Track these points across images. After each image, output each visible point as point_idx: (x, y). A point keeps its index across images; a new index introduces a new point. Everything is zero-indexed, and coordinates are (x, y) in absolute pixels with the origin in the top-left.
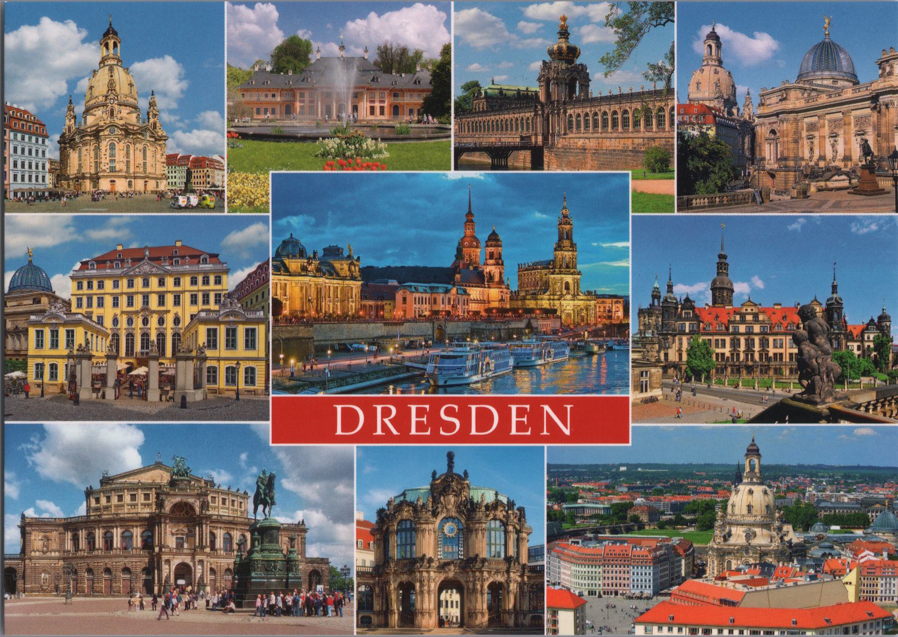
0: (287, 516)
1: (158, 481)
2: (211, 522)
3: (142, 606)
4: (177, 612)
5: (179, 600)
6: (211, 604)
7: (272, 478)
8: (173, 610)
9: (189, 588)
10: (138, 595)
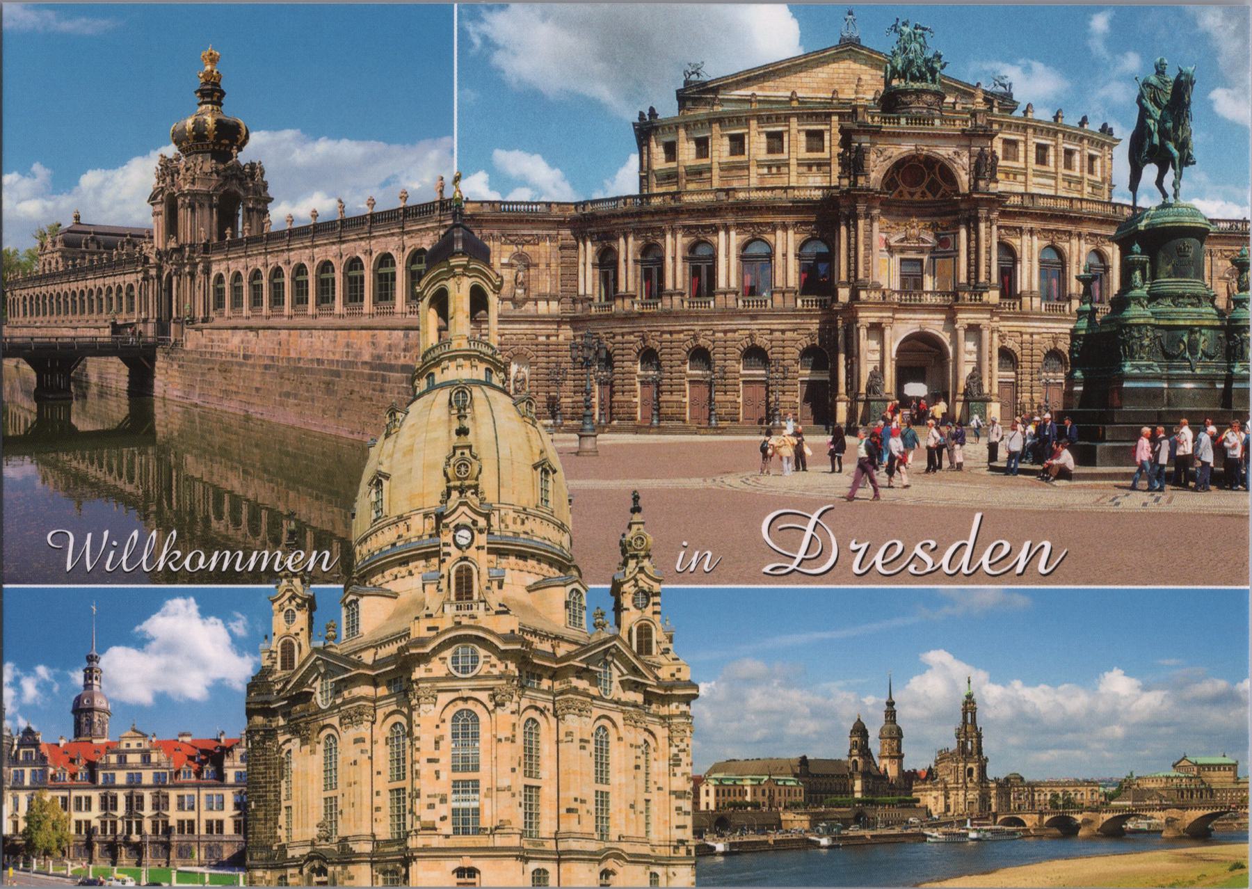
0: (1228, 198)
1: (848, 94)
2: (1004, 214)
3: (800, 461)
4: (902, 477)
5: (910, 442)
6: (1002, 454)
7: (1182, 87)
8: (890, 471)
9: (940, 409)
10: (790, 427)
